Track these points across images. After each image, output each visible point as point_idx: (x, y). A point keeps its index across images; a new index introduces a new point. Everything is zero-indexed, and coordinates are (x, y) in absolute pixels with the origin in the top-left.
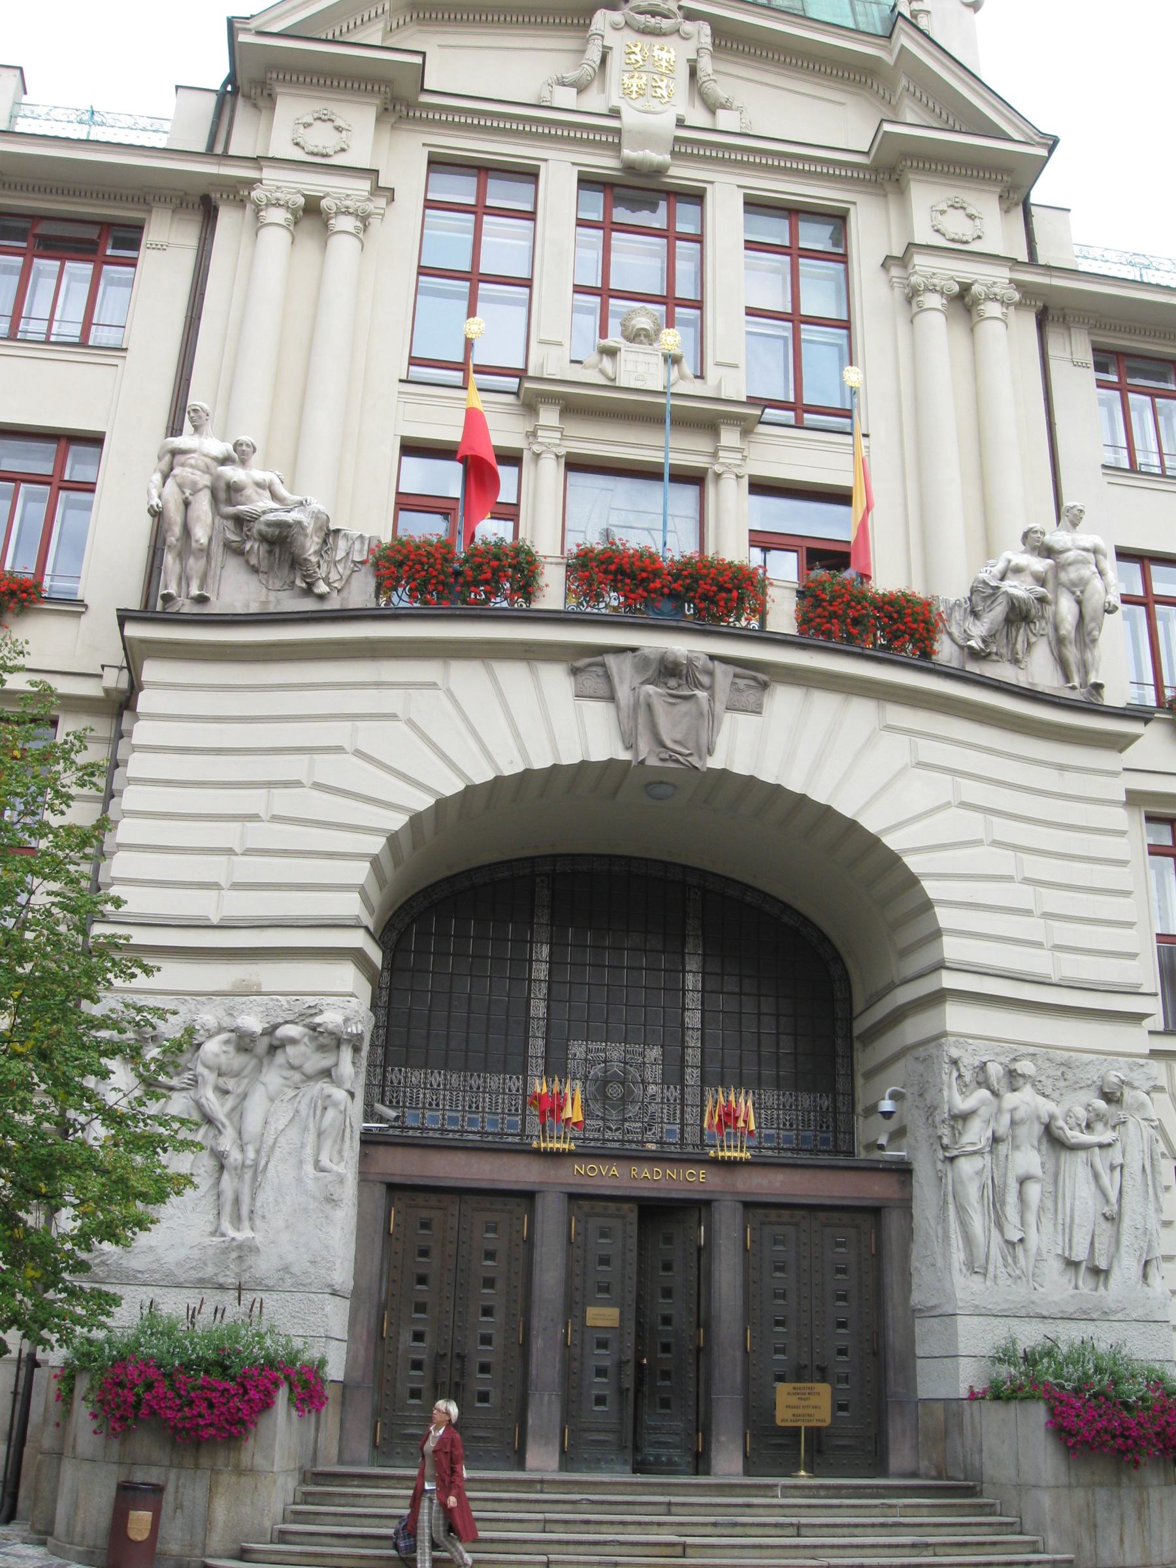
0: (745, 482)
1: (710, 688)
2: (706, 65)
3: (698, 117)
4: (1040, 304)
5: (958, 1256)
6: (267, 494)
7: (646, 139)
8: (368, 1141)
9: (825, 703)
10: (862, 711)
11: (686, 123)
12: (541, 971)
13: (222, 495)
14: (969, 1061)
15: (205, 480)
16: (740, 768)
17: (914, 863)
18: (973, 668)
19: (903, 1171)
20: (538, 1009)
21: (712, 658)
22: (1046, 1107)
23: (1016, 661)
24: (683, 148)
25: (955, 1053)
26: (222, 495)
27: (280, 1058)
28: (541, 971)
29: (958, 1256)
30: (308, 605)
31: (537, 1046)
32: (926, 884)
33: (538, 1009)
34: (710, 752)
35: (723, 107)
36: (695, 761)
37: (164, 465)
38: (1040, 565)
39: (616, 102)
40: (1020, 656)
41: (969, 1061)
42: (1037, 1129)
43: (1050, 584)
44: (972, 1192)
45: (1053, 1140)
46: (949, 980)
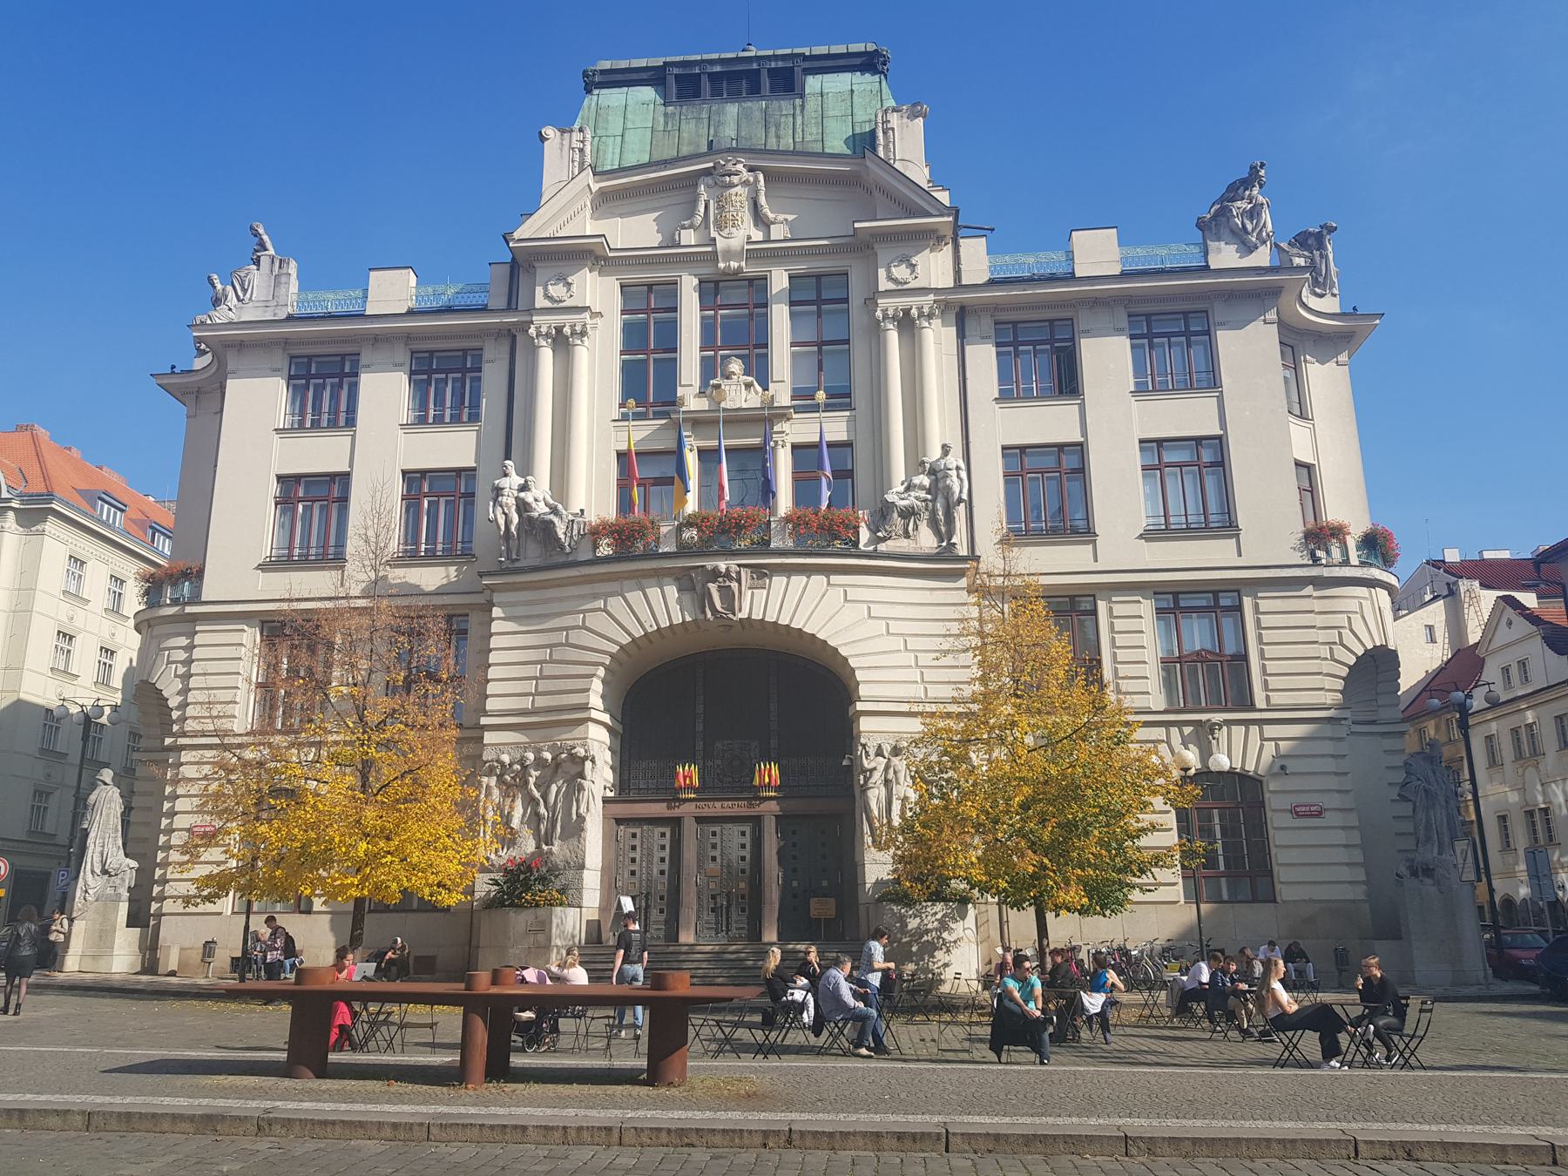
0: (789, 447)
1: (739, 581)
2: (762, 200)
3: (758, 235)
4: (957, 309)
6: (542, 504)
7: (729, 254)
8: (606, 801)
9: (798, 581)
10: (819, 580)
11: (753, 240)
12: (700, 709)
13: (522, 508)
15: (511, 501)
16: (756, 615)
17: (843, 651)
18: (882, 547)
20: (700, 727)
21: (739, 565)
23: (907, 536)
24: (753, 255)
25: (863, 741)
26: (522, 508)
27: (560, 771)
28: (700, 709)
30: (562, 559)
31: (700, 745)
33: (700, 727)
34: (740, 610)
35: (773, 223)
36: (731, 616)
37: (494, 495)
39: (713, 234)
40: (911, 532)
43: (933, 491)
46: (860, 706)
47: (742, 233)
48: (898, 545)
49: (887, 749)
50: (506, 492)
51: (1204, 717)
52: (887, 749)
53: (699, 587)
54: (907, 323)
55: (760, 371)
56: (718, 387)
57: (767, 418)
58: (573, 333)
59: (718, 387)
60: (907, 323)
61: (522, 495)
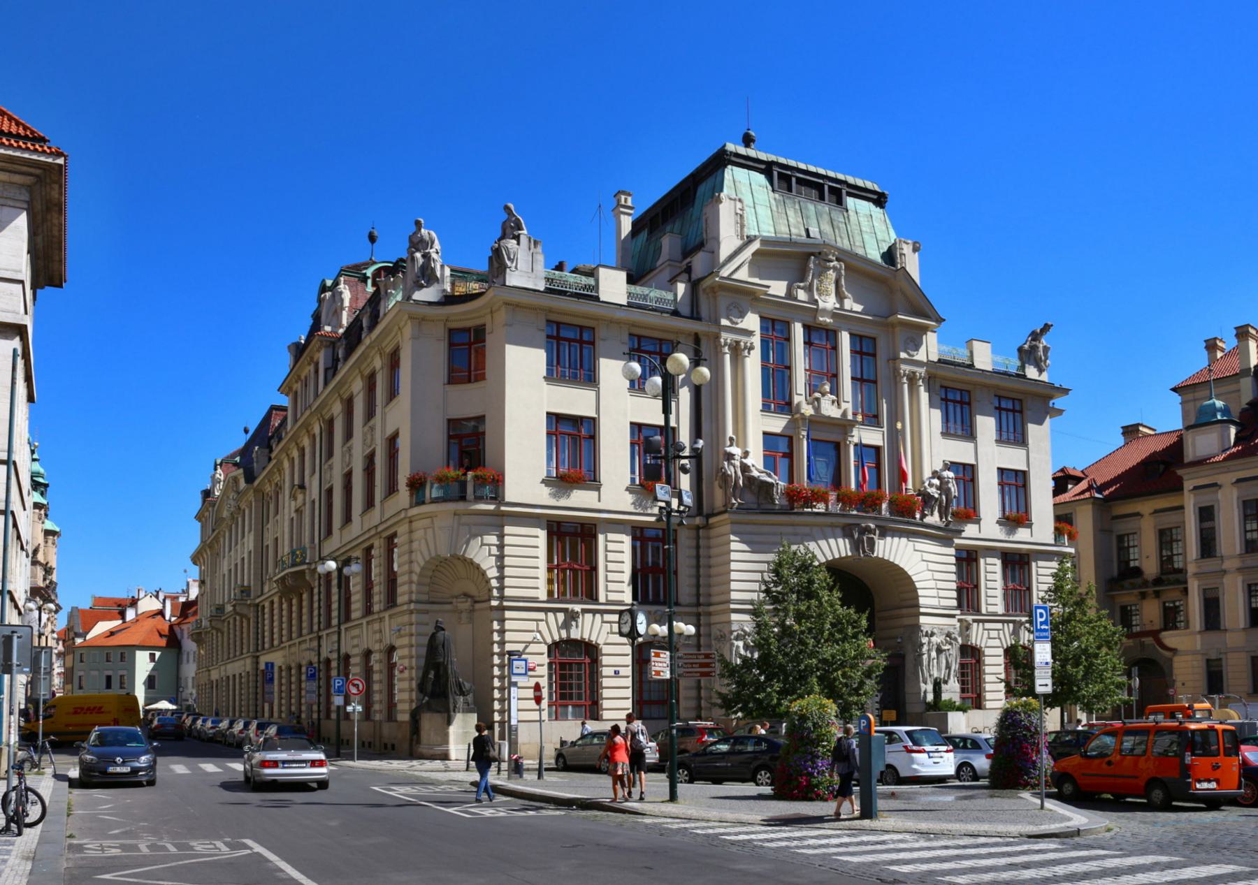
1: (875, 534)
5: (921, 679)
14: (925, 630)
15: (738, 463)
16: (880, 556)
19: (903, 657)
22: (939, 641)
24: (834, 315)
29: (921, 679)
30: (770, 507)
32: (916, 584)
38: (936, 482)
41: (925, 630)
42: (935, 647)
44: (925, 663)
45: (939, 651)
46: (922, 610)
47: (829, 302)
48: (928, 520)
49: (930, 632)
50: (736, 457)
51: (1018, 619)
52: (930, 632)
53: (856, 536)
54: (912, 379)
55: (836, 390)
56: (818, 399)
57: (844, 426)
58: (746, 347)
59: (818, 399)
60: (912, 379)
61: (743, 460)
